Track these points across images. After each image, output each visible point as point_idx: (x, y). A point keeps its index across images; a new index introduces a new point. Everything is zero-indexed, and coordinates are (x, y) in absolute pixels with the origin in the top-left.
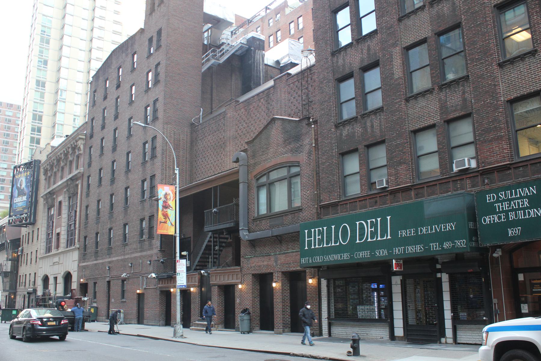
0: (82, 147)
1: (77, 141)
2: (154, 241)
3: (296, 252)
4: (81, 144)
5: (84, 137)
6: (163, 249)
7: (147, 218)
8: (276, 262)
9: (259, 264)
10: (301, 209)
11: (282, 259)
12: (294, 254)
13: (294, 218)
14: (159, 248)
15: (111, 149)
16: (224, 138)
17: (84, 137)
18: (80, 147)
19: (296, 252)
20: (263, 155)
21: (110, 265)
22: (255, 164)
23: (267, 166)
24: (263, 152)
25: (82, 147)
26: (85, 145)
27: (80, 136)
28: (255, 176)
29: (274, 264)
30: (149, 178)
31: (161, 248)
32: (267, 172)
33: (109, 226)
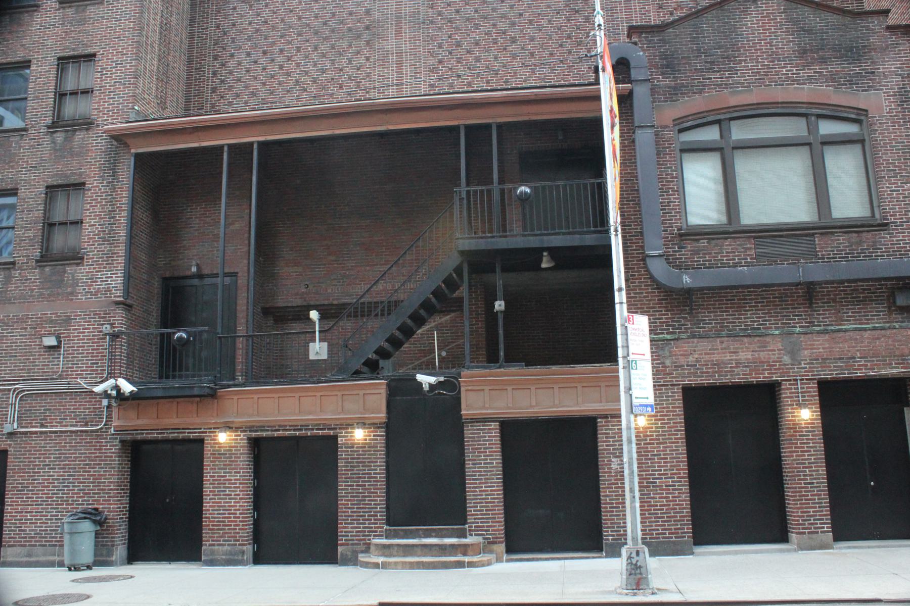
3: (875, 329)
6: (129, 302)
8: (793, 353)
9: (716, 357)
10: (886, 225)
11: (819, 345)
12: (866, 334)
13: (860, 243)
14: (118, 295)
16: (368, 12)
19: (875, 329)
20: (708, 70)
22: (675, 88)
23: (734, 101)
24: (712, 63)
28: (677, 121)
29: (786, 359)
31: (127, 292)
32: (722, 119)
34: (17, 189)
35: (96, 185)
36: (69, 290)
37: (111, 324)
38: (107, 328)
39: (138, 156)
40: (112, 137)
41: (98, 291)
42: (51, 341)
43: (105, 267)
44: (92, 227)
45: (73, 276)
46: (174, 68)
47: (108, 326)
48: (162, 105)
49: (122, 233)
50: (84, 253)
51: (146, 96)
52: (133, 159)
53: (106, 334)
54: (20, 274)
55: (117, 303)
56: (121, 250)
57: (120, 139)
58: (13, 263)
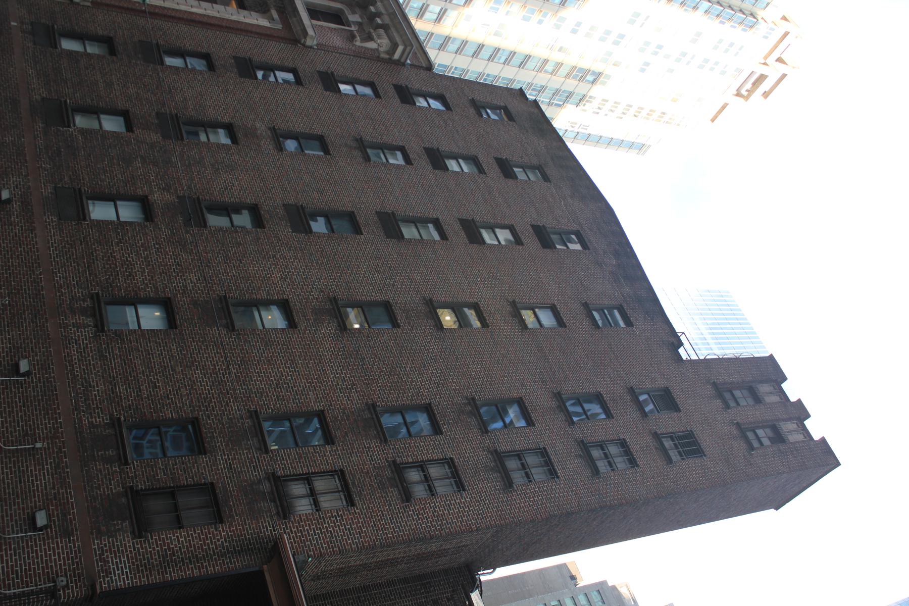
0: (371, 45)
1: (385, 27)
2: (129, 541)
4: (380, 43)
5: (396, 56)
7: (203, 469)
14: (103, 585)
15: (388, 209)
17: (396, 56)
18: (370, 38)
21: (16, 206)
25: (371, 45)
26: (374, 57)
27: (400, 49)
30: (340, 464)
33: (156, 197)
34: (205, 454)
35: (223, 534)
36: (103, 528)
37: (67, 586)
38: (62, 581)
39: (261, 573)
40: (276, 543)
41: (106, 562)
42: (41, 519)
43: (133, 564)
44: (178, 540)
45: (119, 530)
46: (356, 577)
47: (64, 583)
48: (316, 578)
49: (174, 575)
50: (146, 538)
51: (323, 564)
52: (257, 569)
53: (54, 581)
54: (116, 471)
55: (93, 586)
56: (156, 578)
57: (274, 551)
58: (127, 463)
